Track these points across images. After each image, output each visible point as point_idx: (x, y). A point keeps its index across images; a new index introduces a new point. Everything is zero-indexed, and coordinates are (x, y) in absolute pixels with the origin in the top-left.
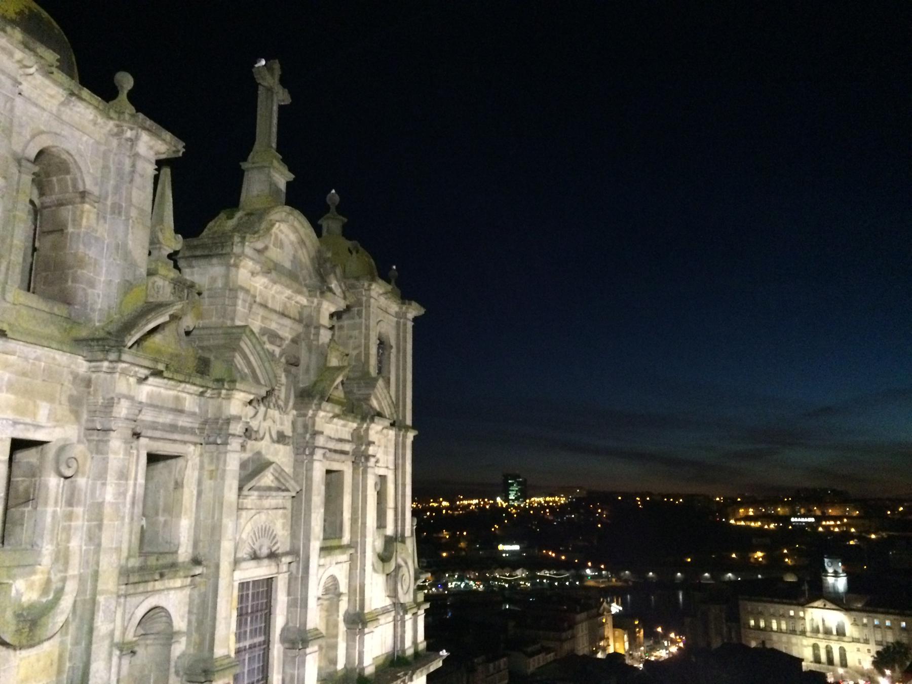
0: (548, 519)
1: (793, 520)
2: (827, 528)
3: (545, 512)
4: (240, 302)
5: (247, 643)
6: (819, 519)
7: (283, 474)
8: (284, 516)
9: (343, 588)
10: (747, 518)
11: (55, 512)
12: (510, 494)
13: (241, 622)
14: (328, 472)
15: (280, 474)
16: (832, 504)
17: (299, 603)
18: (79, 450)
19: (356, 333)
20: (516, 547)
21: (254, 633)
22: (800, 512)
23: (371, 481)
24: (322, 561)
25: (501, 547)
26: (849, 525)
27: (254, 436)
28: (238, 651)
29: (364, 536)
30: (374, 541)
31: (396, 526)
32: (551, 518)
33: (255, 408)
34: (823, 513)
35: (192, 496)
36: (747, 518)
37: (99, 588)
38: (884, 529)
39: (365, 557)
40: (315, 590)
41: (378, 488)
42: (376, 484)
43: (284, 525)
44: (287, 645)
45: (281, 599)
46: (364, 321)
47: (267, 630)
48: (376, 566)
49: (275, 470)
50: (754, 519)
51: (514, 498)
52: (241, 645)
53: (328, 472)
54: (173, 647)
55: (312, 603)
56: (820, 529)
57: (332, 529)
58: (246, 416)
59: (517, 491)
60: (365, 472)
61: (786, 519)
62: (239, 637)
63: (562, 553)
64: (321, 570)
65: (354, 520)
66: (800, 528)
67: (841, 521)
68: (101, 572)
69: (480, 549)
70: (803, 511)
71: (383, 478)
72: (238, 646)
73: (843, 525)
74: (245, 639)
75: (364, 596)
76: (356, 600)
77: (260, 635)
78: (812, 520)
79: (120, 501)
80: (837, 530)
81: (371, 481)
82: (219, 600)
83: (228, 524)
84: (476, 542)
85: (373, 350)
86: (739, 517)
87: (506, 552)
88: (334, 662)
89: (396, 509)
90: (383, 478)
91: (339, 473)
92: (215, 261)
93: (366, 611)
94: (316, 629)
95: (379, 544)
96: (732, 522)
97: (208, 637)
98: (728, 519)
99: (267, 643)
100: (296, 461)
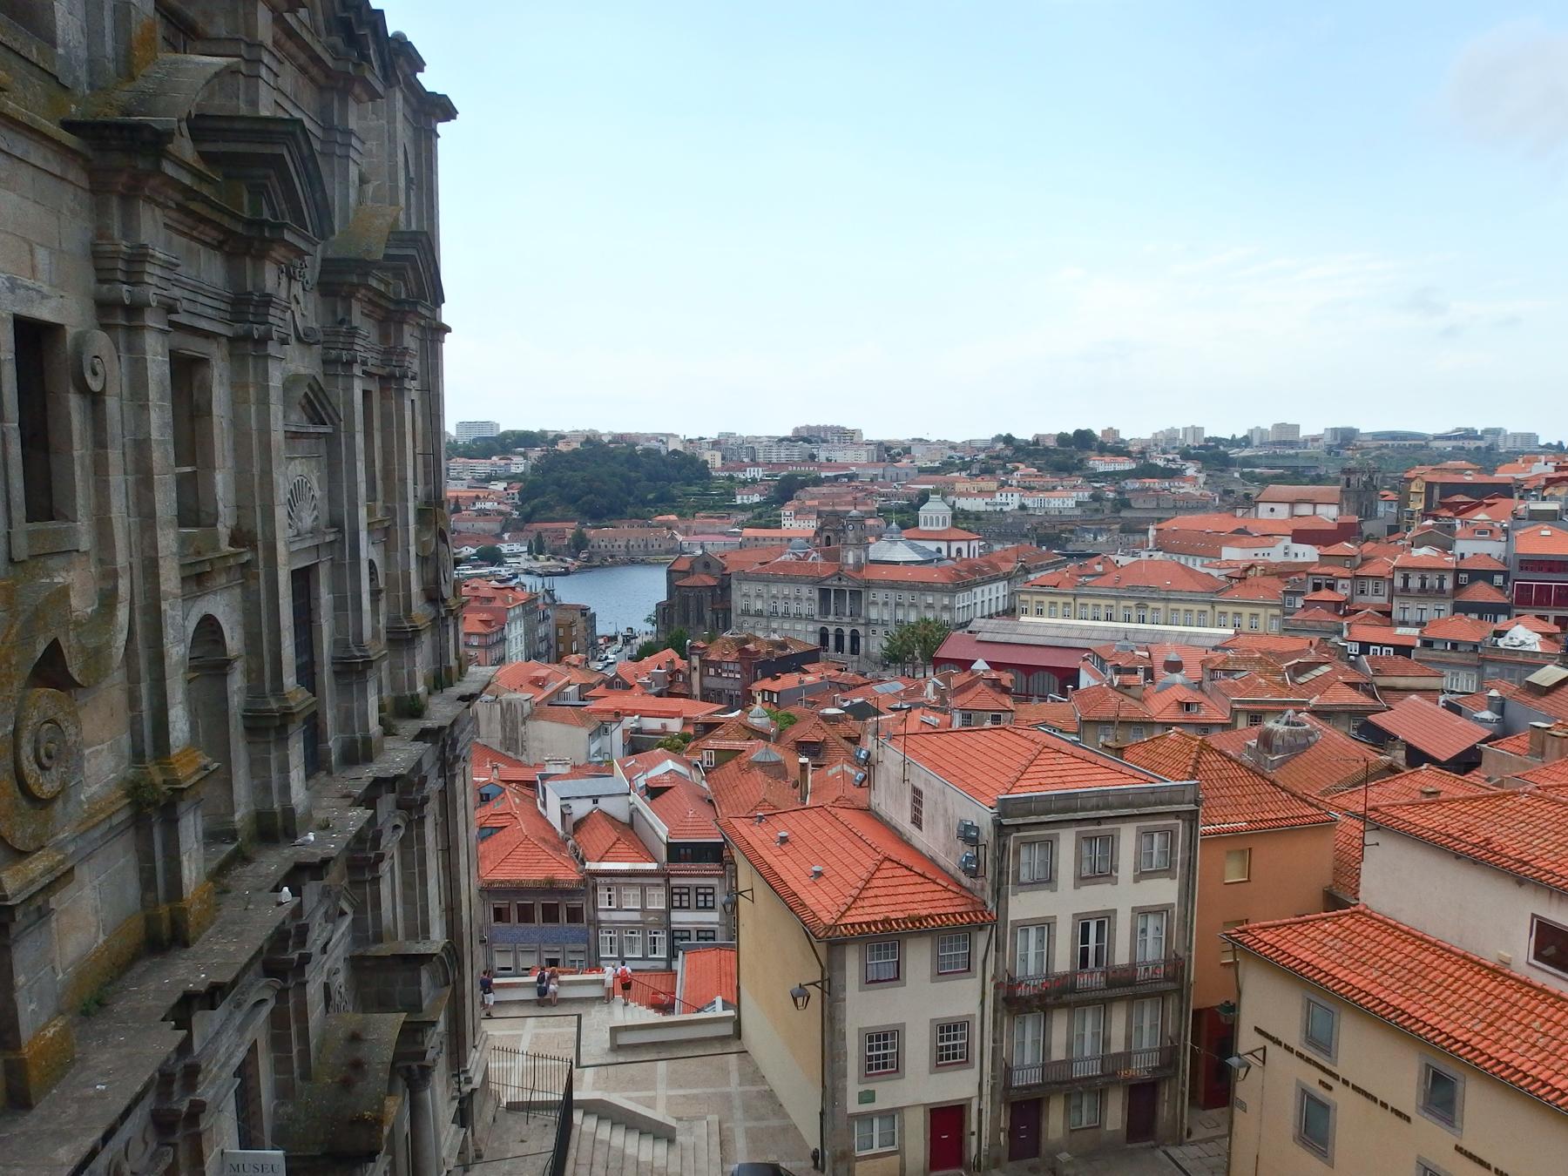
7: (321, 395)
15: (316, 396)
31: (426, 483)
37: (163, 588)
44: (338, 668)
76: (398, 596)
83: (278, 477)
97: (267, 658)
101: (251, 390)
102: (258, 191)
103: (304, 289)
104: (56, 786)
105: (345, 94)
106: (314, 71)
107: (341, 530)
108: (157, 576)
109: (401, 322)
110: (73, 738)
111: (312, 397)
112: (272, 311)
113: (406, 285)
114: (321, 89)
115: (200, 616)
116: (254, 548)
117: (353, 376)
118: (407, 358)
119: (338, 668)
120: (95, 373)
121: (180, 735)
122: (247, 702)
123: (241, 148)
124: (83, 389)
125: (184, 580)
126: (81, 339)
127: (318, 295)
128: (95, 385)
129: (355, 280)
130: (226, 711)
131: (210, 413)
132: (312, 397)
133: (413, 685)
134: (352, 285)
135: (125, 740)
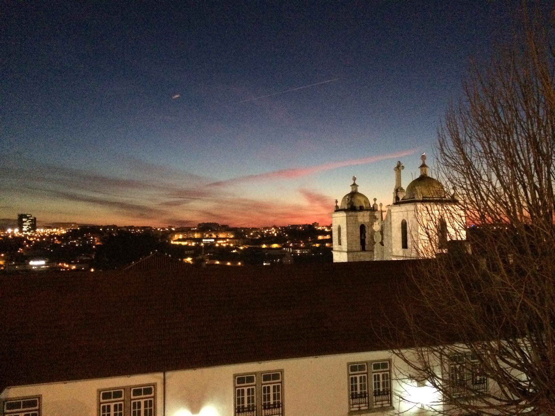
0: (57, 243)
1: (204, 240)
2: (220, 244)
3: (54, 240)
6: (217, 239)
10: (179, 240)
12: (23, 228)
16: (221, 232)
20: (42, 262)
22: (206, 236)
25: (32, 263)
26: (229, 243)
32: (59, 243)
34: (217, 236)
36: (179, 240)
38: (246, 244)
50: (183, 240)
51: (26, 230)
56: (217, 245)
59: (28, 225)
61: (199, 240)
63: (73, 264)
66: (206, 244)
67: (226, 240)
69: (15, 265)
70: (207, 236)
73: (227, 242)
78: (213, 240)
80: (224, 245)
84: (11, 260)
86: (175, 240)
87: (35, 266)
96: (172, 242)
98: (169, 241)
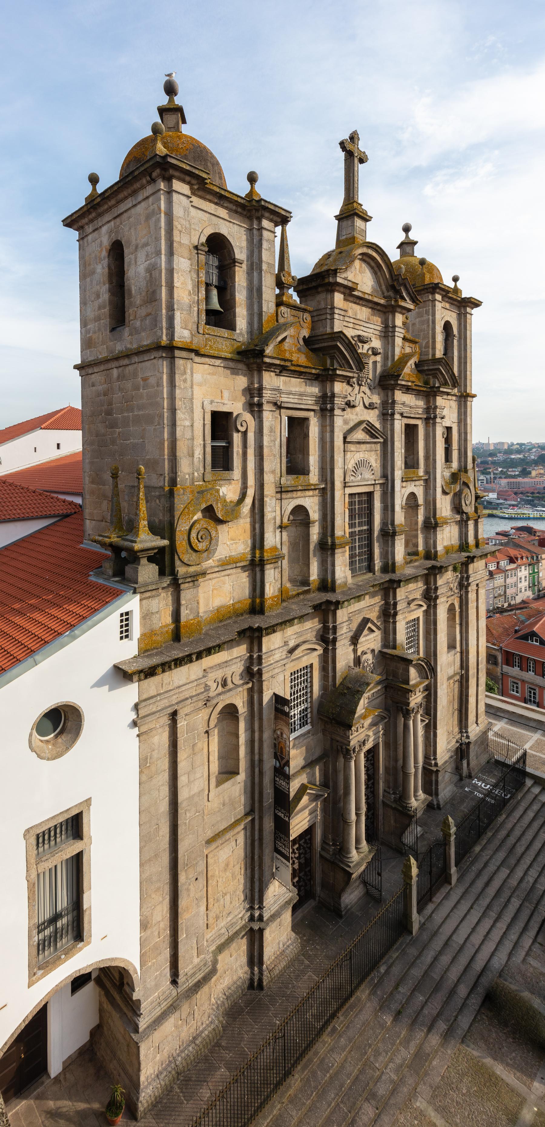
4: (336, 316)
5: (357, 529)
8: (377, 455)
9: (421, 500)
11: (238, 451)
13: (352, 517)
14: (407, 426)
15: (371, 428)
17: (388, 507)
18: (248, 417)
19: (425, 327)
21: (360, 524)
23: (439, 431)
24: (404, 484)
27: (352, 404)
28: (352, 534)
29: (435, 468)
30: (442, 472)
33: (352, 386)
35: (315, 442)
39: (436, 481)
40: (400, 500)
41: (445, 436)
42: (443, 434)
43: (376, 460)
44: (383, 533)
45: (377, 505)
46: (430, 317)
47: (370, 522)
48: (444, 487)
49: (367, 424)
52: (353, 530)
53: (407, 426)
54: (311, 529)
55: (398, 508)
57: (411, 463)
58: (346, 391)
60: (434, 424)
62: (351, 526)
64: (403, 490)
65: (427, 458)
68: (265, 485)
71: (449, 429)
72: (351, 530)
74: (355, 527)
75: (436, 506)
77: (365, 525)
79: (272, 444)
81: (439, 431)
82: (336, 503)
85: (440, 338)
88: (416, 545)
89: (459, 450)
90: (449, 429)
91: (416, 426)
92: (320, 289)
93: (437, 516)
94: (401, 524)
95: (447, 474)
99: (370, 531)
100: (383, 419)
101: (328, 427)
102: (332, 358)
103: (370, 389)
104: (204, 548)
105: (393, 312)
106: (379, 308)
107: (387, 479)
108: (263, 489)
109: (435, 396)
110: (214, 535)
111: (369, 428)
112: (336, 399)
113: (438, 380)
114: (385, 313)
115: (295, 505)
116: (326, 484)
117: (387, 420)
118: (438, 410)
119: (383, 533)
120: (242, 426)
121: (270, 543)
122: (322, 539)
123: (326, 344)
124: (238, 431)
125: (277, 492)
126: (238, 416)
127: (380, 390)
128: (242, 429)
129: (392, 382)
130: (309, 540)
131: (308, 436)
132: (369, 428)
133: (435, 546)
134: (392, 385)
135: (249, 542)
